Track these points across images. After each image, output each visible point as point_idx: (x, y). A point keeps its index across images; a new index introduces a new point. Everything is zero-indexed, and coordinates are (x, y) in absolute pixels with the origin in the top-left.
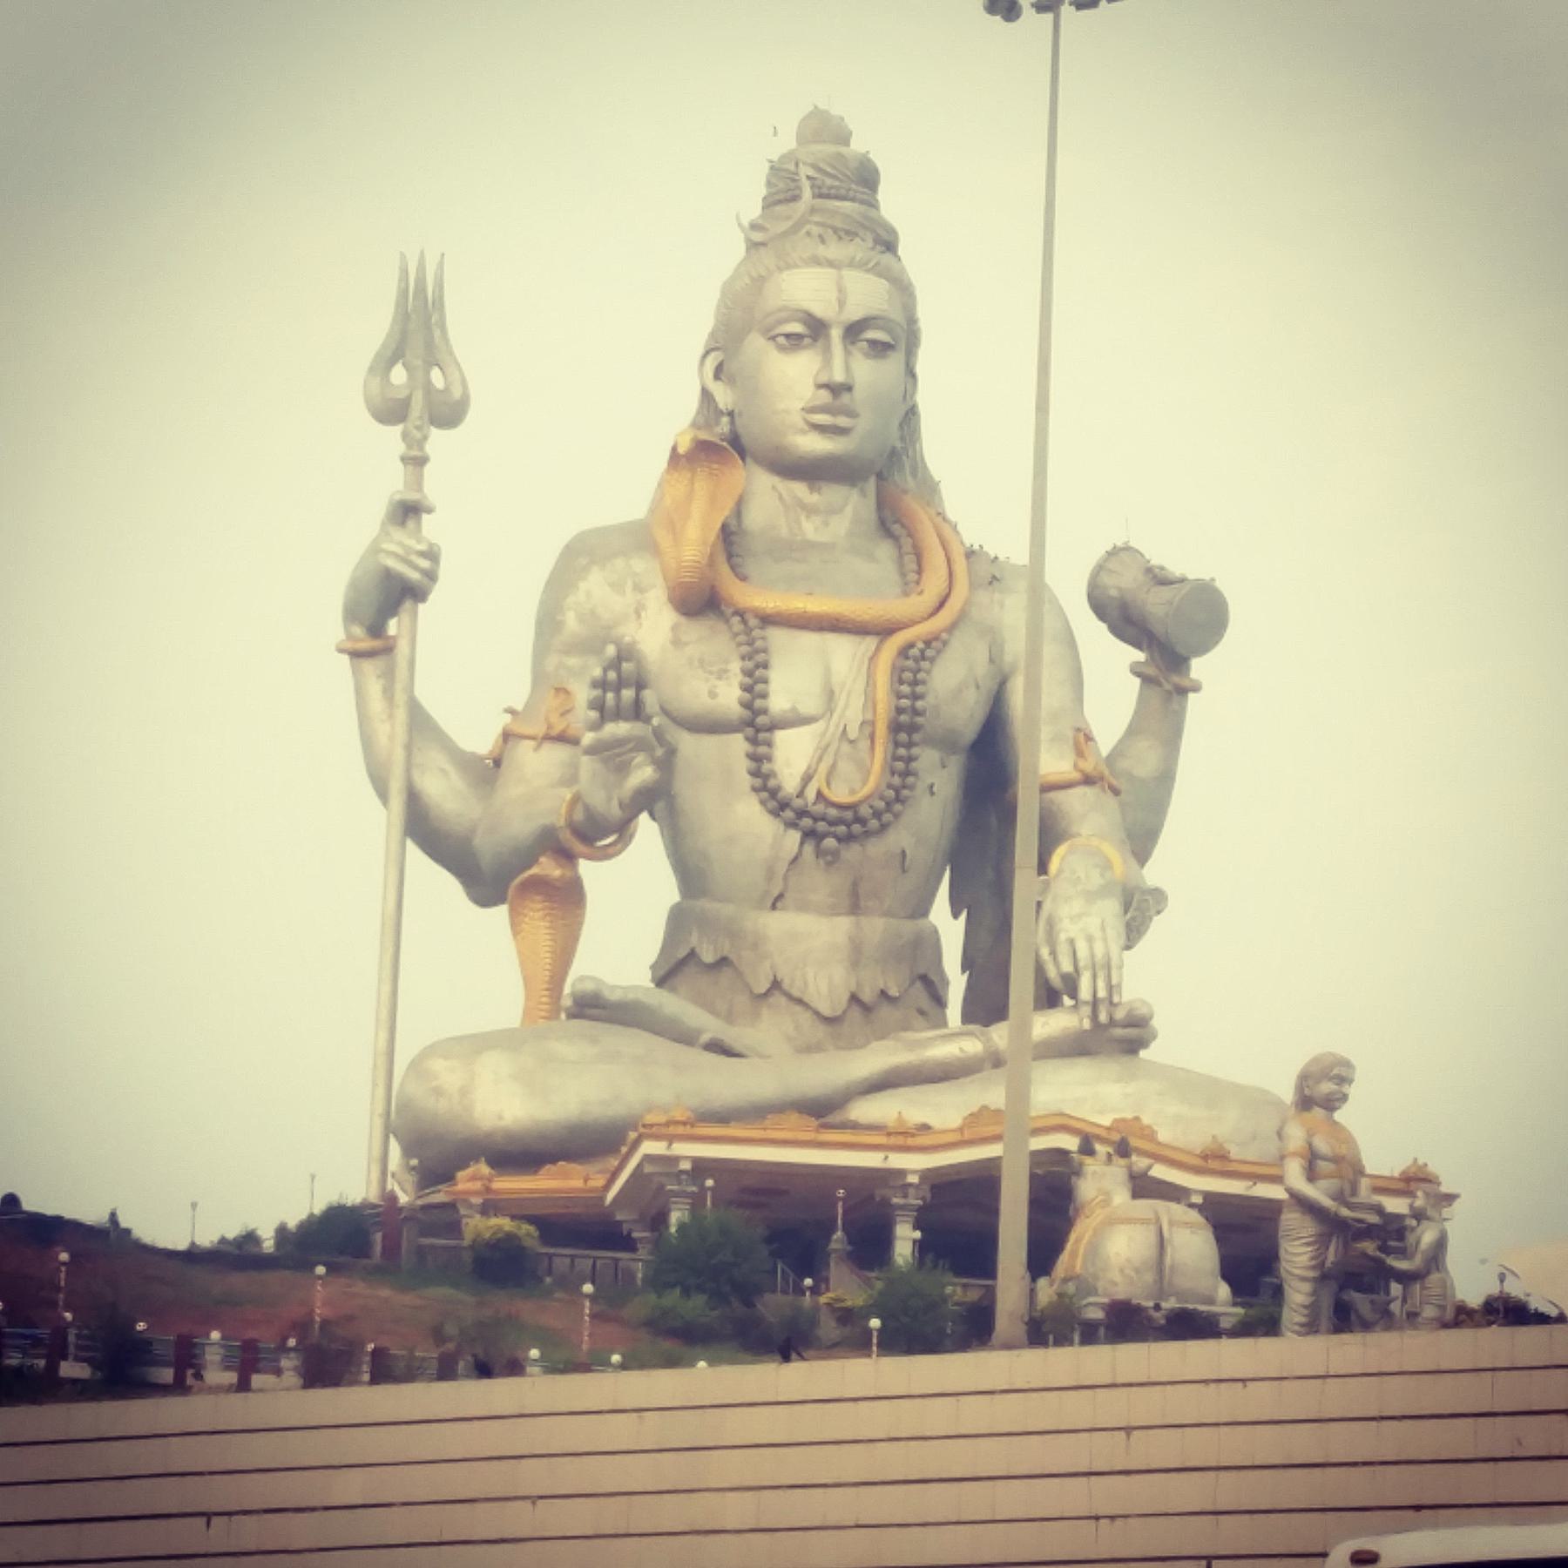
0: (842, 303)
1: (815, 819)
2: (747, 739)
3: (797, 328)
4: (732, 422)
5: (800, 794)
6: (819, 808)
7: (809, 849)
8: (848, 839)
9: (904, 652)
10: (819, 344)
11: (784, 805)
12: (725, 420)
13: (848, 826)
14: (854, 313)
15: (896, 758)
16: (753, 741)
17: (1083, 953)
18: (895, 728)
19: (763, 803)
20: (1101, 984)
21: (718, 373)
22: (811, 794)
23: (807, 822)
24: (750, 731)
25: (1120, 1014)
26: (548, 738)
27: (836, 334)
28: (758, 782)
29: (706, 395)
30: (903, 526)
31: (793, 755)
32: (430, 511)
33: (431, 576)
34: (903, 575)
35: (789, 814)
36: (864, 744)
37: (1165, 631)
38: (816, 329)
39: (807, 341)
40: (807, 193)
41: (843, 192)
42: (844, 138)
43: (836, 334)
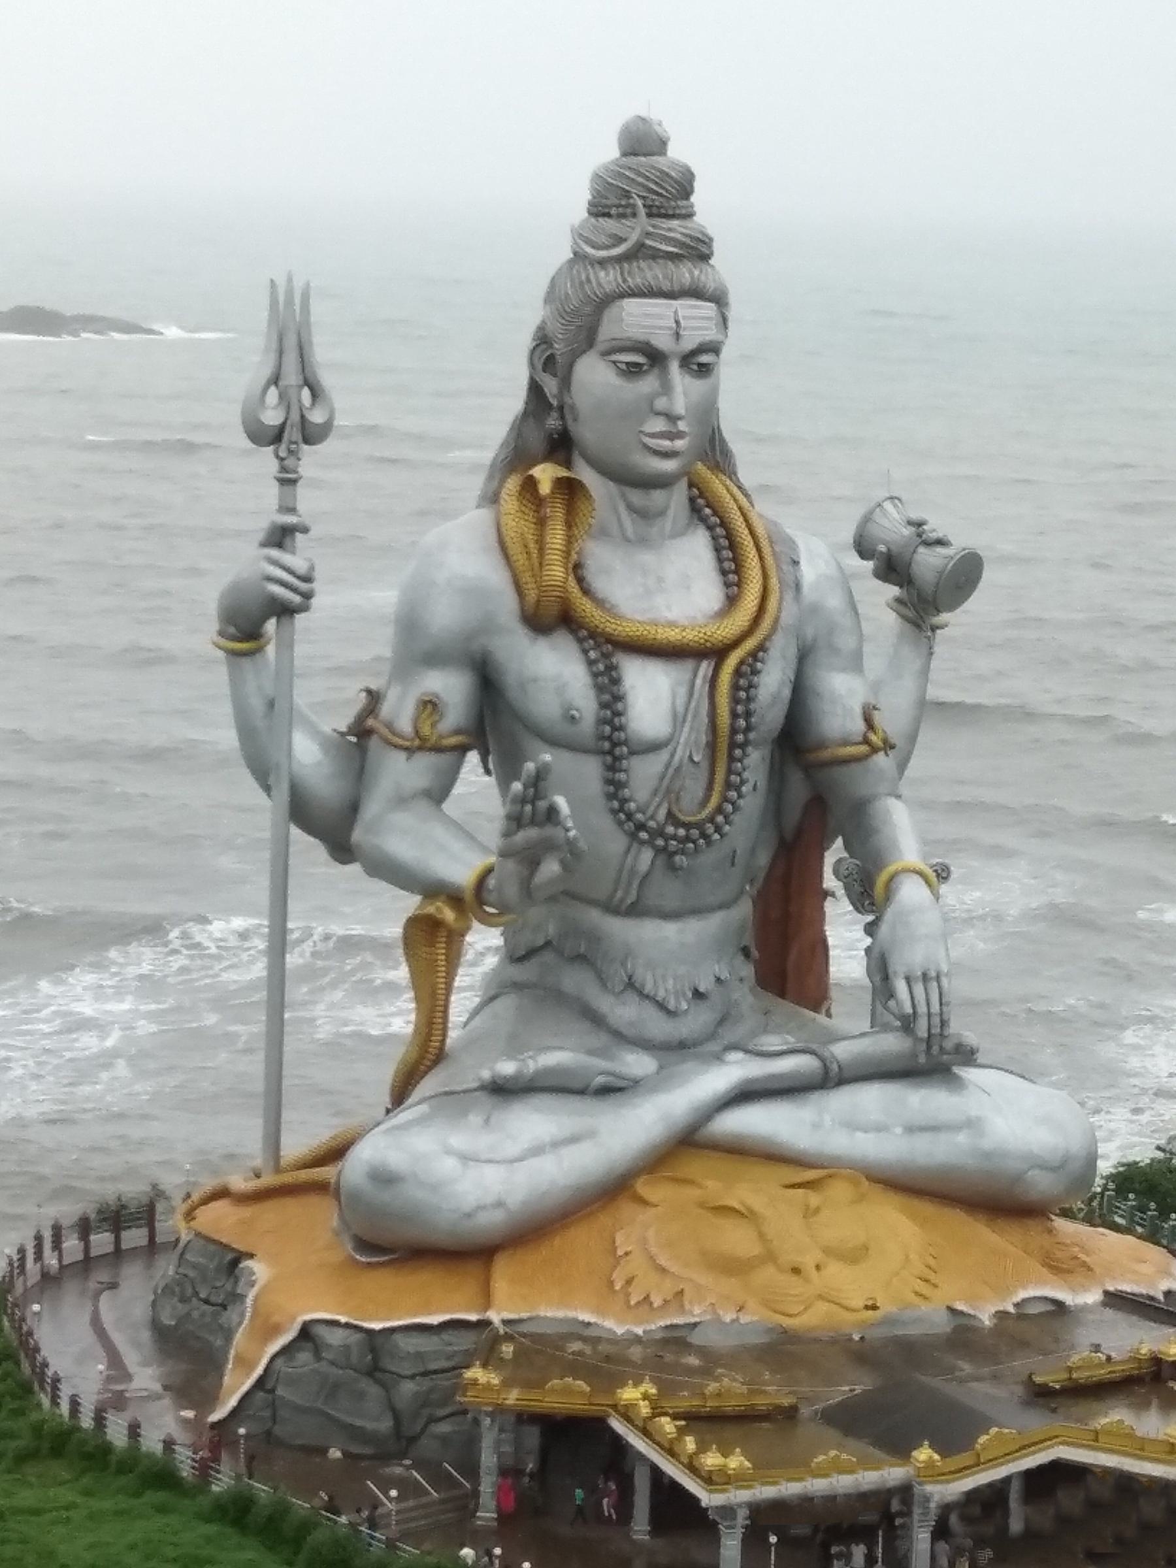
0: (677, 336)
1: (666, 840)
2: (604, 764)
3: (640, 359)
4: (562, 417)
5: (652, 818)
6: (670, 829)
7: (659, 862)
8: (697, 850)
9: (738, 673)
10: (656, 371)
11: (641, 827)
12: (555, 414)
13: (694, 842)
14: (688, 345)
15: (730, 771)
16: (612, 768)
17: (919, 989)
18: (733, 745)
19: (620, 824)
20: (936, 1021)
21: (549, 364)
22: (662, 814)
23: (660, 842)
24: (609, 759)
25: (949, 1045)
26: (420, 748)
27: (674, 366)
28: (616, 804)
29: (535, 390)
30: (715, 513)
31: (644, 775)
32: (305, 530)
33: (307, 596)
34: (724, 573)
35: (644, 835)
36: (705, 765)
37: (923, 585)
38: (655, 358)
39: (645, 368)
40: (642, 211)
41: (671, 212)
42: (661, 146)
43: (674, 366)
